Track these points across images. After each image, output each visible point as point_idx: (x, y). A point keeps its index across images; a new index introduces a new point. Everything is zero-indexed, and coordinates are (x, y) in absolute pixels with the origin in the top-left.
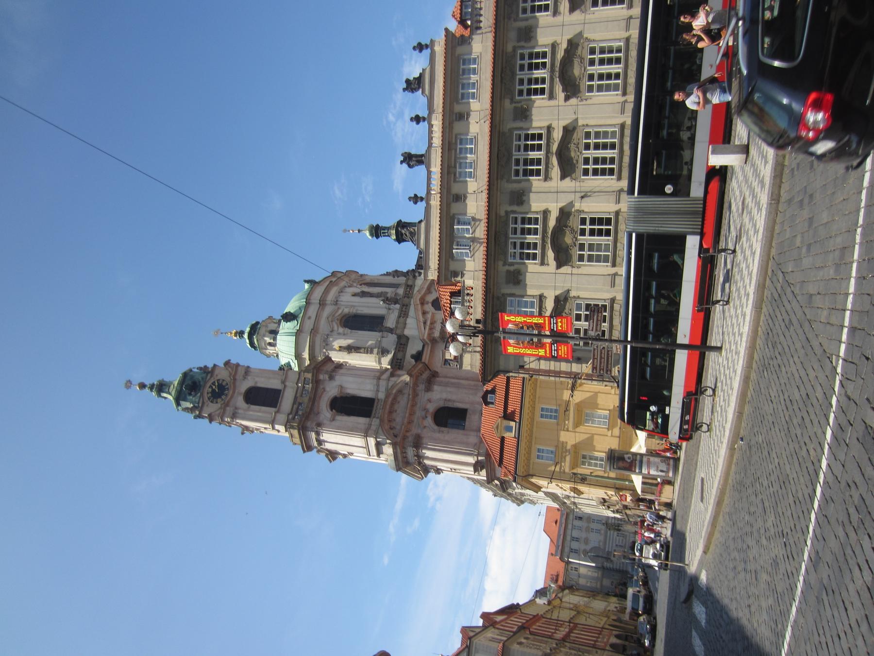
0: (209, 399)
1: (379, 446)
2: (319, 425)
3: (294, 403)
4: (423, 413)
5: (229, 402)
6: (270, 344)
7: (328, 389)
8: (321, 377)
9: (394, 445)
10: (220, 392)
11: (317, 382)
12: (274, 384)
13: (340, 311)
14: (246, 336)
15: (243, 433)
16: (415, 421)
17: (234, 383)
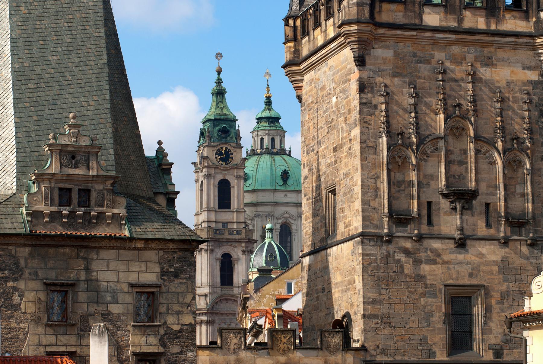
0: (218, 150)
1: (206, 296)
2: (212, 251)
3: (223, 223)
4: (228, 321)
5: (218, 168)
6: (262, 139)
7: (236, 249)
8: (243, 245)
9: (208, 310)
10: (225, 157)
11: (240, 241)
12: (234, 204)
13: (292, 221)
14: (267, 114)
15: (192, 163)
16: (222, 318)
17: (231, 168)
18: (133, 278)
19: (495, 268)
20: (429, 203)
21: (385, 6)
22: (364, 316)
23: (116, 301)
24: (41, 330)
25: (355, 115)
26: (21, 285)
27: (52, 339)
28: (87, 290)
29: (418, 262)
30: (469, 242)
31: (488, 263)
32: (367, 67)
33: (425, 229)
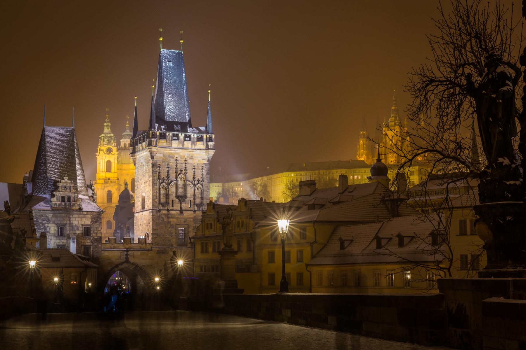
18: (83, 223)
19: (192, 220)
20: (173, 200)
21: (161, 141)
22: (152, 234)
23: (78, 230)
24: (55, 238)
25: (151, 174)
26: (50, 225)
27: (58, 241)
28: (69, 226)
29: (168, 218)
30: (184, 212)
31: (189, 218)
32: (155, 159)
33: (171, 208)
